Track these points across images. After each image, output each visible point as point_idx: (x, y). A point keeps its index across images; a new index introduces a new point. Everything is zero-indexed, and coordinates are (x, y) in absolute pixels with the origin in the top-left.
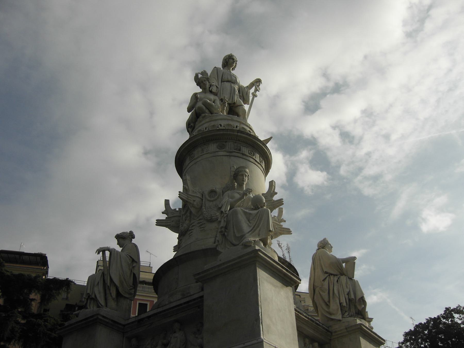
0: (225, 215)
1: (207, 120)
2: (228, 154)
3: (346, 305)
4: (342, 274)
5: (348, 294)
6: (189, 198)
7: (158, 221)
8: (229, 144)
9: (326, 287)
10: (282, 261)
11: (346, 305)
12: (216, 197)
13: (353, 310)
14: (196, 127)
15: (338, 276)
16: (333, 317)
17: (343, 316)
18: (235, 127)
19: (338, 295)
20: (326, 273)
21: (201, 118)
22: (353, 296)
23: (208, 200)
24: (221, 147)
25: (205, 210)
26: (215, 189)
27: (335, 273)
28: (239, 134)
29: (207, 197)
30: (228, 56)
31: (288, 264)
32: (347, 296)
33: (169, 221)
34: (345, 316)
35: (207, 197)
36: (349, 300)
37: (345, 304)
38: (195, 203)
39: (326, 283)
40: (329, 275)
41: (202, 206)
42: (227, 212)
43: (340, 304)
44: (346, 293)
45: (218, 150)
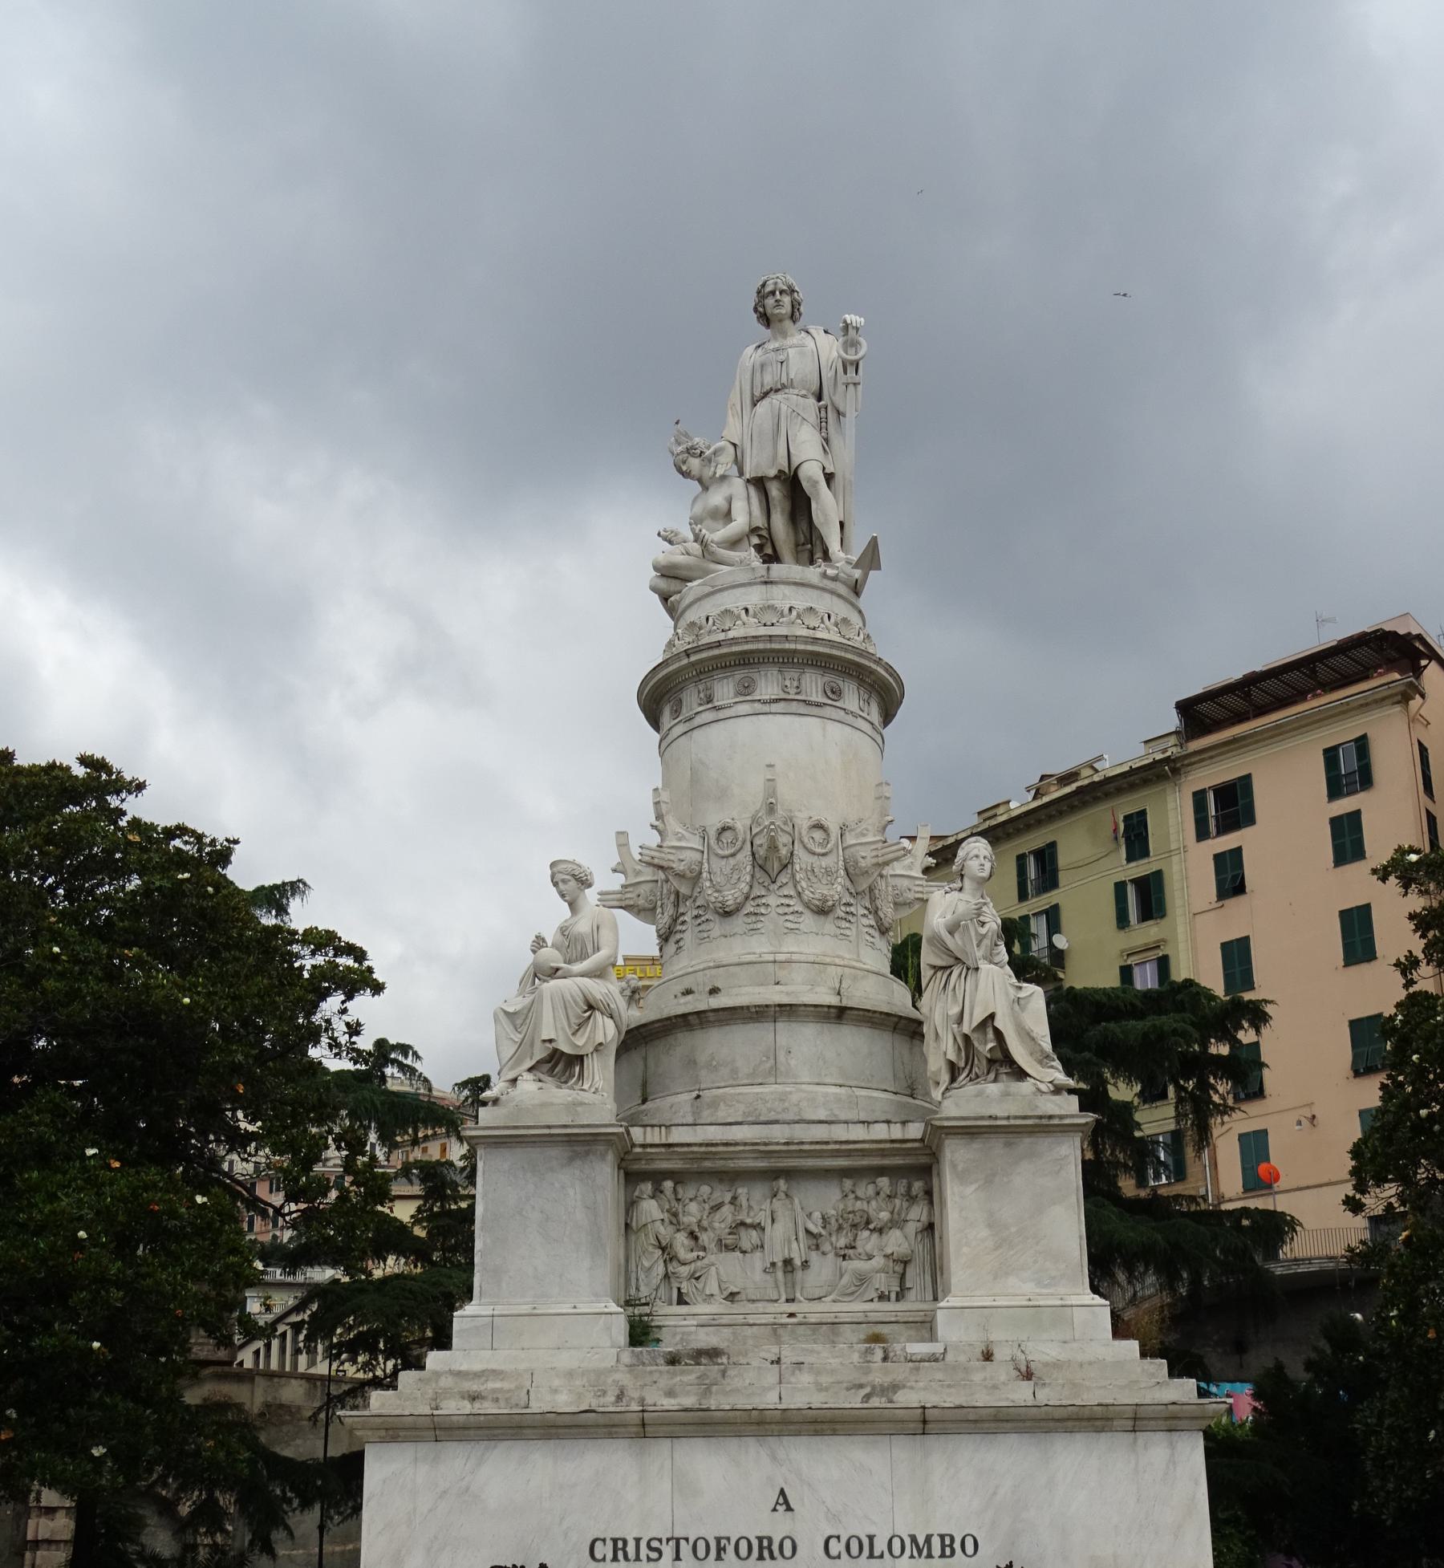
10: (754, 1010)
28: (693, 658)
31: (777, 1009)
38: (641, 902)
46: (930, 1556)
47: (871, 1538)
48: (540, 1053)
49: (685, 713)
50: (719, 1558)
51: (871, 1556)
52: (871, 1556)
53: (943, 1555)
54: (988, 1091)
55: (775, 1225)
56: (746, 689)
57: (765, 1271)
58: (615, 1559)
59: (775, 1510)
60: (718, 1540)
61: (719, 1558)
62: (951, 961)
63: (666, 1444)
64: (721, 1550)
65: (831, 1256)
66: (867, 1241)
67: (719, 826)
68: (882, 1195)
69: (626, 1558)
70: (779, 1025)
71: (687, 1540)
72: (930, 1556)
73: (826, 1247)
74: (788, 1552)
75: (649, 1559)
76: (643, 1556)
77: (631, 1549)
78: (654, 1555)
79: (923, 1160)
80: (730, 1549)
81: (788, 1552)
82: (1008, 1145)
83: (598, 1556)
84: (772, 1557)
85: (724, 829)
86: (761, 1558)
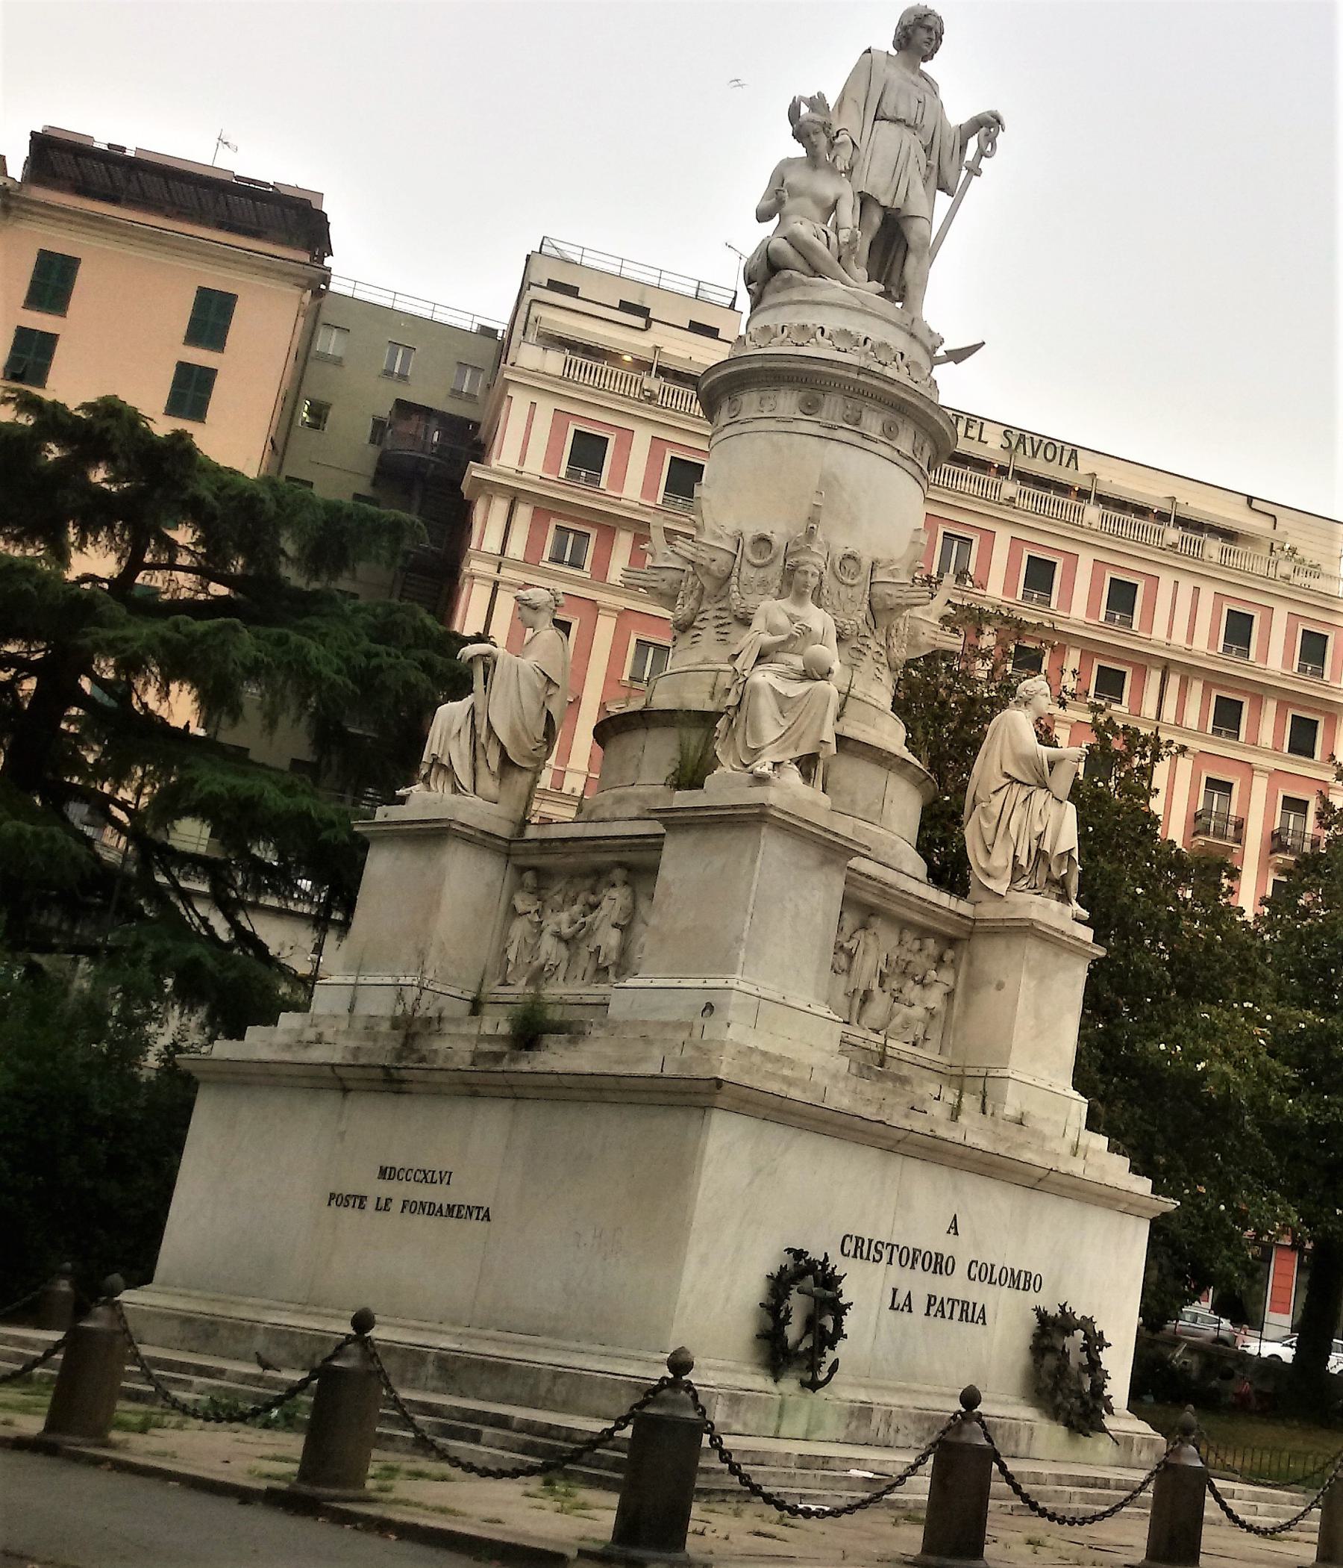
0: (741, 680)
1: (796, 295)
2: (823, 432)
3: (1025, 865)
4: (1044, 786)
5: (1040, 837)
6: (701, 554)
7: (629, 574)
8: (833, 399)
9: (995, 810)
11: (1025, 865)
12: (770, 557)
13: (1042, 875)
14: (768, 300)
15: (1031, 789)
16: (990, 884)
17: (1013, 886)
18: (862, 341)
19: (1015, 839)
20: (1008, 776)
21: (776, 281)
22: (1047, 848)
23: (748, 561)
24: (810, 407)
25: (735, 588)
26: (769, 534)
27: (1025, 781)
28: (862, 378)
29: (748, 551)
30: (913, 18)
32: (1034, 843)
33: (654, 578)
34: (1017, 888)
35: (748, 551)
36: (1038, 850)
37: (1023, 861)
38: (714, 567)
39: (998, 800)
40: (1012, 783)
41: (729, 577)
42: (746, 673)
43: (1015, 857)
44: (1034, 836)
45: (799, 415)
46: (1018, 1288)
47: (993, 1266)
48: (805, 750)
49: (823, 416)
50: (913, 1267)
51: (990, 1282)
52: (990, 1282)
53: (1024, 1289)
54: (1051, 906)
55: (866, 958)
56: (890, 432)
57: (846, 994)
58: (855, 1256)
59: (949, 1232)
60: (915, 1251)
61: (913, 1267)
62: (1033, 781)
63: (900, 1158)
64: (915, 1260)
65: (887, 994)
66: (912, 991)
67: (848, 551)
68: (926, 952)
69: (861, 1257)
70: (891, 774)
71: (898, 1246)
72: (1018, 1288)
73: (886, 987)
74: (949, 1271)
75: (874, 1260)
76: (871, 1258)
77: (865, 1248)
78: (877, 1257)
79: (963, 935)
80: (920, 1260)
81: (949, 1271)
82: (1057, 955)
83: (846, 1252)
84: (941, 1273)
85: (849, 557)
86: (935, 1272)
